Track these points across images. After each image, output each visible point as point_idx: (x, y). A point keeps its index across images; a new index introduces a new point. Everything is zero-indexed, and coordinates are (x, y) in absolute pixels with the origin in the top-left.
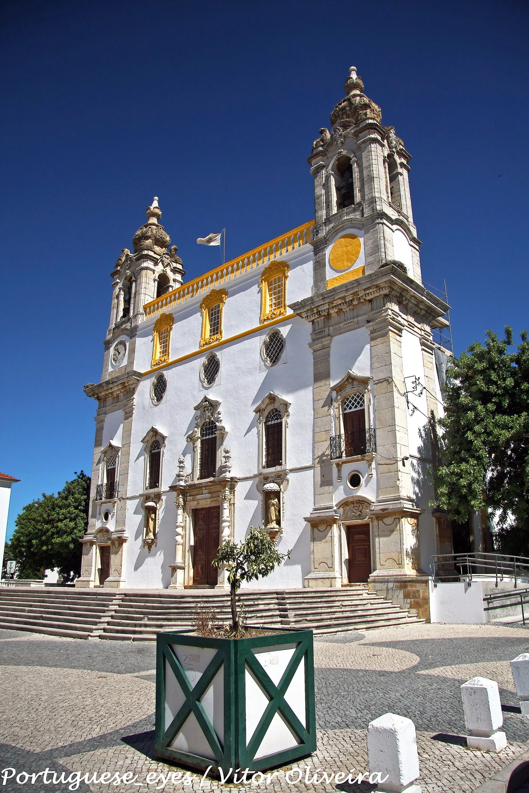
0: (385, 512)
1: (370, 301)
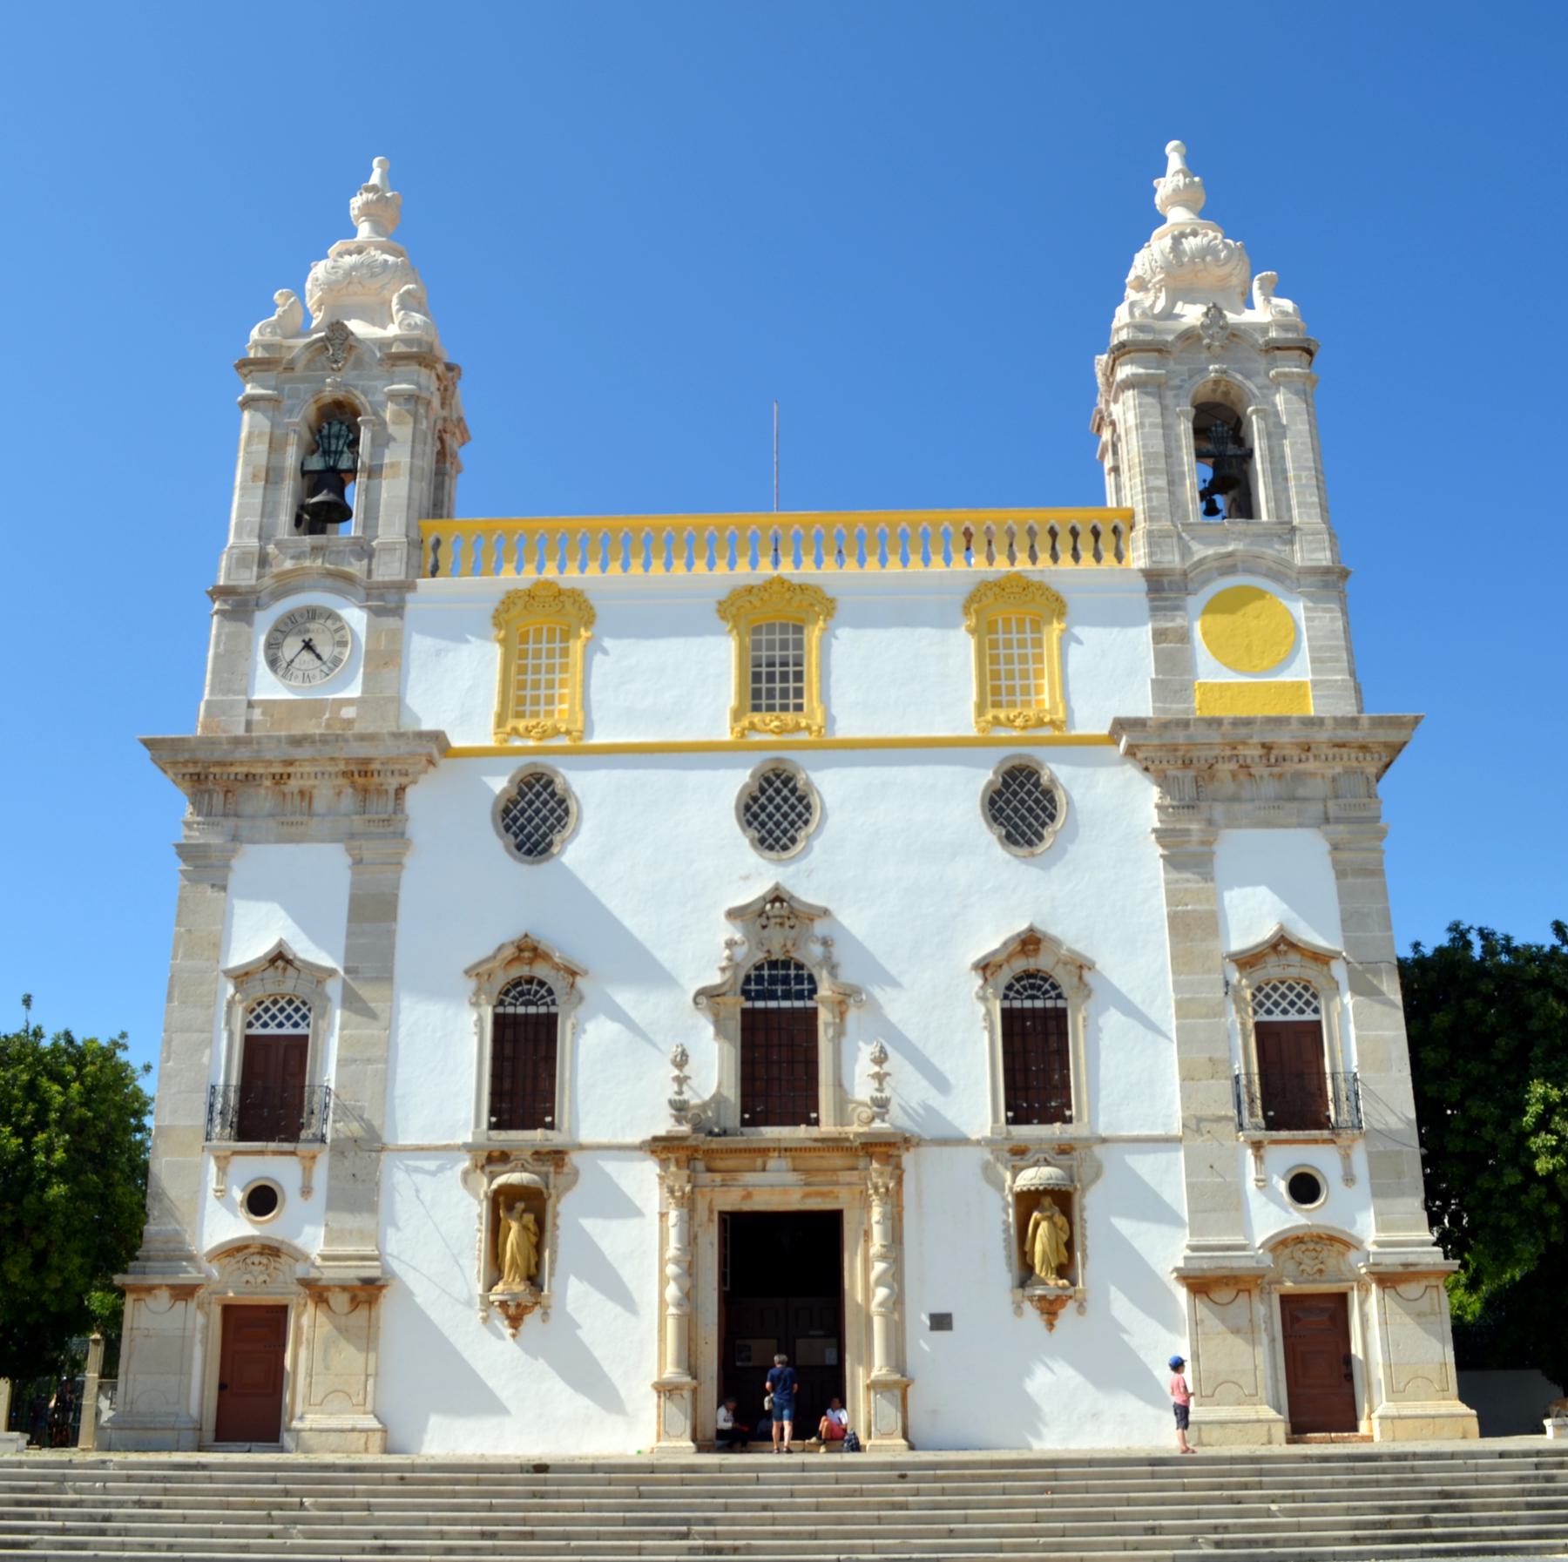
0: (1412, 1269)
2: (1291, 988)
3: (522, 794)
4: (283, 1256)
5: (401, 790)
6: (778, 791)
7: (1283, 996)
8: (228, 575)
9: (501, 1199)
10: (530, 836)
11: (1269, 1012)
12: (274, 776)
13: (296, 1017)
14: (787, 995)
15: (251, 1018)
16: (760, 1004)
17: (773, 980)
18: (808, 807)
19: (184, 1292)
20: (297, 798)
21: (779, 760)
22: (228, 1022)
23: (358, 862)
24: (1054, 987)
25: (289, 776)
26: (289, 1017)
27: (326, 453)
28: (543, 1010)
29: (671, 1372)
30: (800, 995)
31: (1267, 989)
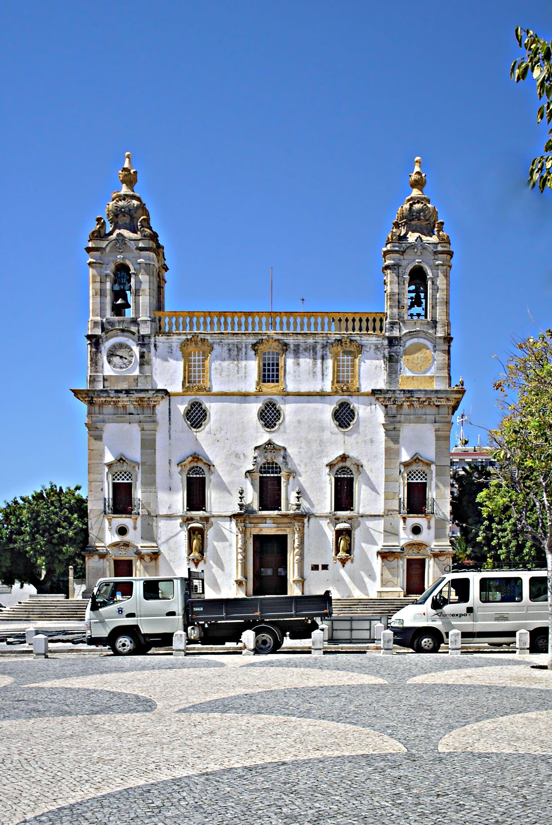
1: (437, 406)
2: (419, 473)
3: (192, 408)
4: (130, 547)
5: (154, 406)
6: (271, 409)
7: (417, 475)
8: (92, 330)
9: (191, 531)
10: (195, 422)
11: (412, 479)
12: (114, 401)
13: (128, 477)
14: (273, 473)
15: (114, 477)
16: (265, 475)
17: (269, 468)
18: (280, 414)
19: (102, 556)
20: (122, 408)
21: (271, 399)
22: (107, 479)
23: (143, 430)
24: (351, 471)
25: (119, 401)
26: (125, 477)
27: (120, 284)
28: (201, 476)
29: (240, 577)
30: (276, 473)
31: (412, 473)
